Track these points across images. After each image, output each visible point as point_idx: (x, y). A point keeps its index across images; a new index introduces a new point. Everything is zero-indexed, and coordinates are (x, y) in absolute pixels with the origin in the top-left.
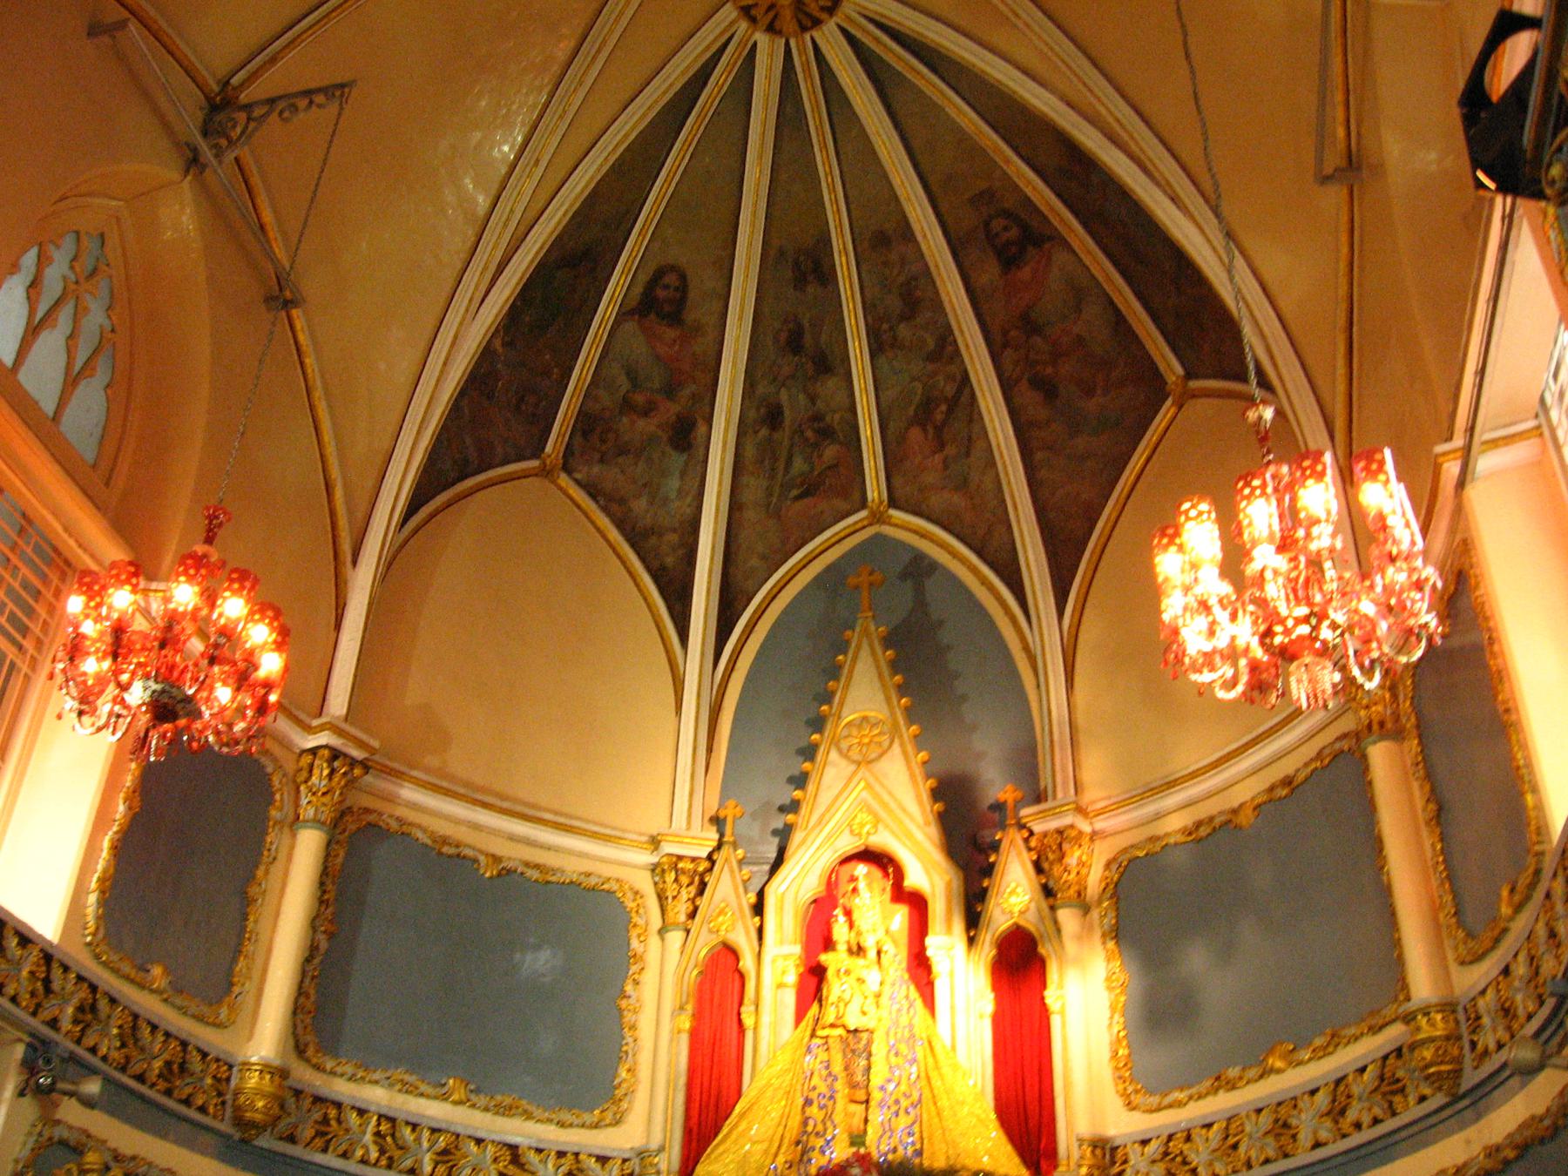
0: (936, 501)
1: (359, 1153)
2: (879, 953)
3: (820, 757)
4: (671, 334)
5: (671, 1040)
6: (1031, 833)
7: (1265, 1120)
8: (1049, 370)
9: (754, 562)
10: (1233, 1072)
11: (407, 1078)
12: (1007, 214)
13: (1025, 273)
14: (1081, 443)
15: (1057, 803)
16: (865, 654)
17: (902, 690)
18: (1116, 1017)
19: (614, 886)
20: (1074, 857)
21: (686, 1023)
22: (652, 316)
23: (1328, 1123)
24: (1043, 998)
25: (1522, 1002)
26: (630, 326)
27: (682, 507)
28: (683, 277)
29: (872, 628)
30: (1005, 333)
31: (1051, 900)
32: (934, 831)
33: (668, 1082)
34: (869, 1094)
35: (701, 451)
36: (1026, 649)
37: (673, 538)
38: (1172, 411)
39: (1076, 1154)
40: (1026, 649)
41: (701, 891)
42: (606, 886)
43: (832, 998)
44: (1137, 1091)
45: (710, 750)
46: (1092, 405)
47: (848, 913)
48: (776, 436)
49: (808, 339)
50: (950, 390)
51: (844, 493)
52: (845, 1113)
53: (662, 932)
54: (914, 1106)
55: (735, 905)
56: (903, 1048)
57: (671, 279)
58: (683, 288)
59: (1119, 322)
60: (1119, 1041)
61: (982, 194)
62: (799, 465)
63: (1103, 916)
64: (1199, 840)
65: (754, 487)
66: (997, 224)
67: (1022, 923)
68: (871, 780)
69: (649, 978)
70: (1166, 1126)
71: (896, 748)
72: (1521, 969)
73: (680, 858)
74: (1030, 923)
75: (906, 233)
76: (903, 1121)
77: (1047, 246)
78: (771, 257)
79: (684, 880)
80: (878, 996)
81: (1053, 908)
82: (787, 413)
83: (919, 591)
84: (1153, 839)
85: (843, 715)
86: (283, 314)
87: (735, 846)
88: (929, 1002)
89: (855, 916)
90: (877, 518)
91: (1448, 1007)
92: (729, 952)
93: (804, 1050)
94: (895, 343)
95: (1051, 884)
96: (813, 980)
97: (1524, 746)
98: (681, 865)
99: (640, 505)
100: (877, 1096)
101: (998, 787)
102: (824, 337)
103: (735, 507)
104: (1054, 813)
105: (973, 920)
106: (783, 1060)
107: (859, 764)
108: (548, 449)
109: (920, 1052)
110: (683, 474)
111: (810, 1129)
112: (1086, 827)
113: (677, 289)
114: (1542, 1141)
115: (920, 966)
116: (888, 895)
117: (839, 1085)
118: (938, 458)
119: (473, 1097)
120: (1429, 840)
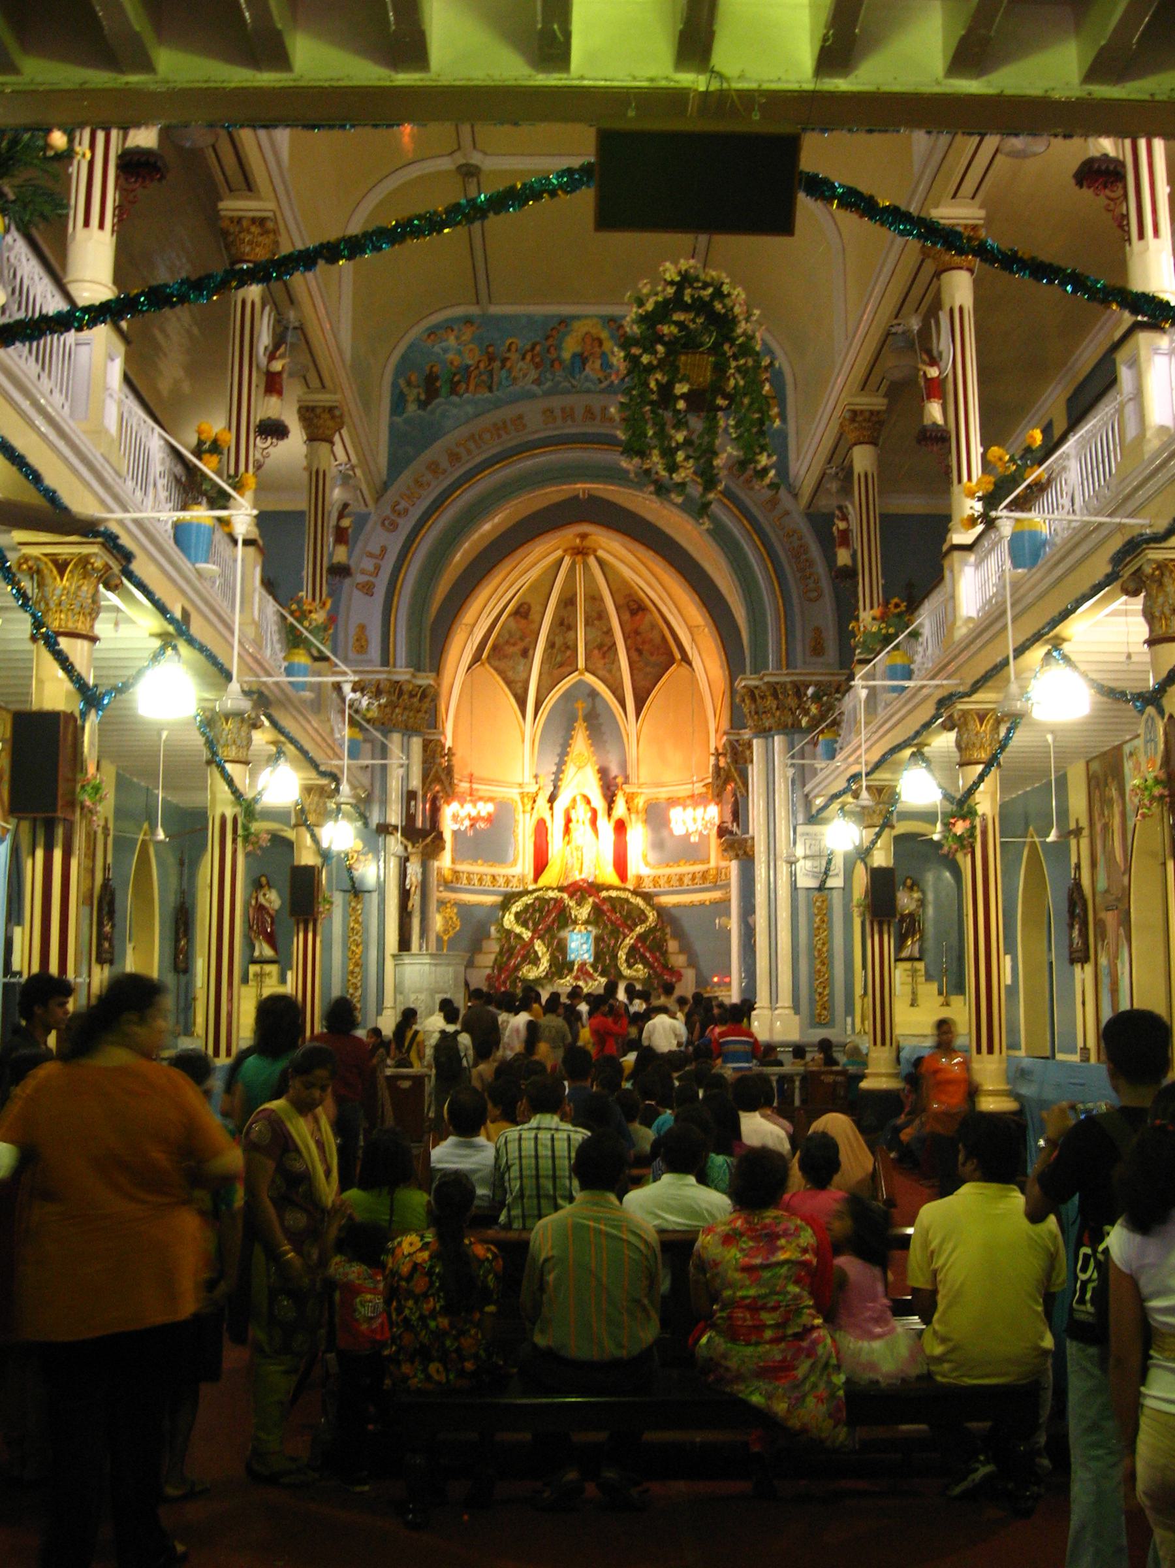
4: (523, 621)
13: (638, 618)
14: (648, 669)
17: (592, 745)
20: (636, 801)
27: (524, 676)
37: (520, 685)
41: (534, 801)
46: (653, 659)
49: (566, 622)
50: (609, 644)
51: (571, 665)
63: (642, 816)
65: (546, 667)
66: (631, 603)
75: (602, 600)
83: (594, 704)
90: (581, 674)
94: (593, 625)
96: (567, 830)
99: (510, 674)
101: (614, 770)
105: (609, 815)
118: (602, 662)
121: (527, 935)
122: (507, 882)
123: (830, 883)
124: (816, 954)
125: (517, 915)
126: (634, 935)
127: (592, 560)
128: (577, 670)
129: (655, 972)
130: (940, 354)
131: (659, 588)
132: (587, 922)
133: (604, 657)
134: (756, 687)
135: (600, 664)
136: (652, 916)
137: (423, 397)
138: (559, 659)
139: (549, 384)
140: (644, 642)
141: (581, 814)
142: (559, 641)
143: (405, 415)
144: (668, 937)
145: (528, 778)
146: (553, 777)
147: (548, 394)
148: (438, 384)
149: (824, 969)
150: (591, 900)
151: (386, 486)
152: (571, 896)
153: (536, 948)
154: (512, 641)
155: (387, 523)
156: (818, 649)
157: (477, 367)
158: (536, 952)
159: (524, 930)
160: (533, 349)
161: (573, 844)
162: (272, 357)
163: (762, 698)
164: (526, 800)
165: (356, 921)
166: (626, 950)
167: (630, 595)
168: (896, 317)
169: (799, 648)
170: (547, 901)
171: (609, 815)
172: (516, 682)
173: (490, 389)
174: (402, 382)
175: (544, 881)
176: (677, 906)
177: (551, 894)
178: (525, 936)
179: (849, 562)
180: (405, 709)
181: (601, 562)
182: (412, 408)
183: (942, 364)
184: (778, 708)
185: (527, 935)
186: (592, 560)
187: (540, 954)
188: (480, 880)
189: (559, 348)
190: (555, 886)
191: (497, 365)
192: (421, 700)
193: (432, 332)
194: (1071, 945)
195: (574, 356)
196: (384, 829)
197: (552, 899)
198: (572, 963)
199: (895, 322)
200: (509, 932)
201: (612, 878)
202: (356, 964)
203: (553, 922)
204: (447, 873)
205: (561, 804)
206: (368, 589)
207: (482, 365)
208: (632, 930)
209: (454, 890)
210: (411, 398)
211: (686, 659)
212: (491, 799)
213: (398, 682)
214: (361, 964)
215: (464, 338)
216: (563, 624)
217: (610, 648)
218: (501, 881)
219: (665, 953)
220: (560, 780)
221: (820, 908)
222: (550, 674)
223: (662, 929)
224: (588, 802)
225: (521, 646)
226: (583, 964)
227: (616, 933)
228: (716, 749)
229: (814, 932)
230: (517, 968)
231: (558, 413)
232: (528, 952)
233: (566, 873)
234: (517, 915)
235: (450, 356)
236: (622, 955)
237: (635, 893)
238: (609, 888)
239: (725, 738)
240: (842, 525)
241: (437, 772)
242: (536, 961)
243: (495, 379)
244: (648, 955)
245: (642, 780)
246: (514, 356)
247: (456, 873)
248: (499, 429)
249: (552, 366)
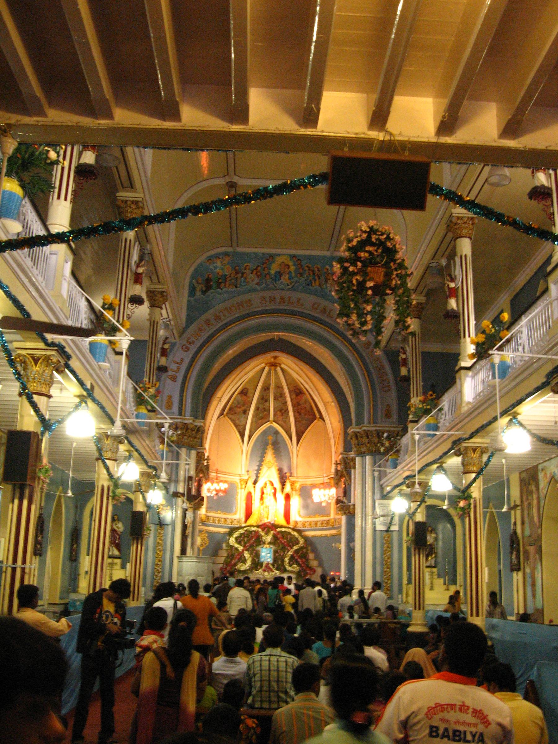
7: (314, 523)
13: (299, 397)
14: (304, 422)
17: (275, 457)
21: (245, 502)
27: (243, 423)
41: (246, 483)
46: (306, 416)
51: (266, 418)
52: (266, 516)
58: (247, 391)
63: (298, 492)
65: (255, 419)
75: (282, 388)
83: (277, 437)
90: (271, 423)
96: (262, 498)
99: (237, 422)
101: (285, 470)
105: (282, 491)
121: (241, 548)
122: (232, 522)
123: (393, 528)
124: (384, 563)
125: (237, 538)
126: (293, 550)
127: (278, 369)
128: (269, 421)
130: (455, 276)
131: (311, 384)
132: (270, 543)
133: (282, 415)
134: (358, 432)
135: (280, 418)
136: (302, 541)
137: (204, 289)
138: (261, 415)
139: (264, 285)
140: (302, 409)
141: (269, 490)
142: (261, 407)
143: (196, 297)
145: (244, 472)
146: (256, 472)
147: (264, 290)
148: (211, 283)
149: (388, 570)
150: (272, 532)
151: (185, 330)
152: (263, 530)
153: (245, 555)
155: (184, 347)
156: (388, 415)
157: (230, 276)
158: (244, 557)
160: (256, 269)
161: (264, 505)
162: (138, 266)
163: (361, 437)
164: (242, 482)
165: (161, 540)
166: (288, 558)
168: (433, 259)
169: (379, 413)
170: (251, 532)
171: (282, 491)
172: (239, 425)
173: (236, 287)
174: (194, 281)
175: (250, 522)
176: (314, 537)
177: (253, 529)
178: (239, 549)
179: (406, 374)
180: (189, 437)
181: (282, 369)
182: (198, 294)
183: (456, 281)
184: (368, 443)
185: (241, 548)
186: (278, 369)
187: (247, 558)
188: (219, 521)
189: (269, 269)
190: (255, 524)
191: (240, 275)
192: (197, 433)
193: (210, 259)
194: (511, 563)
195: (276, 272)
196: (176, 495)
197: (254, 531)
198: (262, 563)
199: (433, 261)
200: (232, 547)
201: (282, 522)
202: (160, 561)
204: (203, 517)
205: (259, 485)
206: (174, 379)
207: (232, 275)
208: (292, 548)
209: (205, 525)
210: (198, 289)
211: (321, 417)
212: (226, 482)
213: (186, 424)
214: (162, 561)
215: (225, 262)
216: (264, 399)
217: (285, 411)
218: (229, 521)
219: (307, 560)
220: (259, 473)
221: (386, 540)
222: (256, 422)
223: (306, 548)
224: (272, 485)
225: (243, 408)
226: (268, 564)
227: (284, 549)
228: (336, 461)
229: (384, 552)
230: (235, 565)
231: (267, 299)
233: (260, 518)
235: (217, 270)
236: (287, 560)
237: (294, 530)
238: (281, 527)
239: (341, 456)
240: (403, 356)
241: (201, 468)
242: (244, 561)
243: (239, 282)
244: (299, 560)
245: (299, 475)
246: (248, 272)
247: (207, 517)
248: (239, 305)
249: (265, 277)
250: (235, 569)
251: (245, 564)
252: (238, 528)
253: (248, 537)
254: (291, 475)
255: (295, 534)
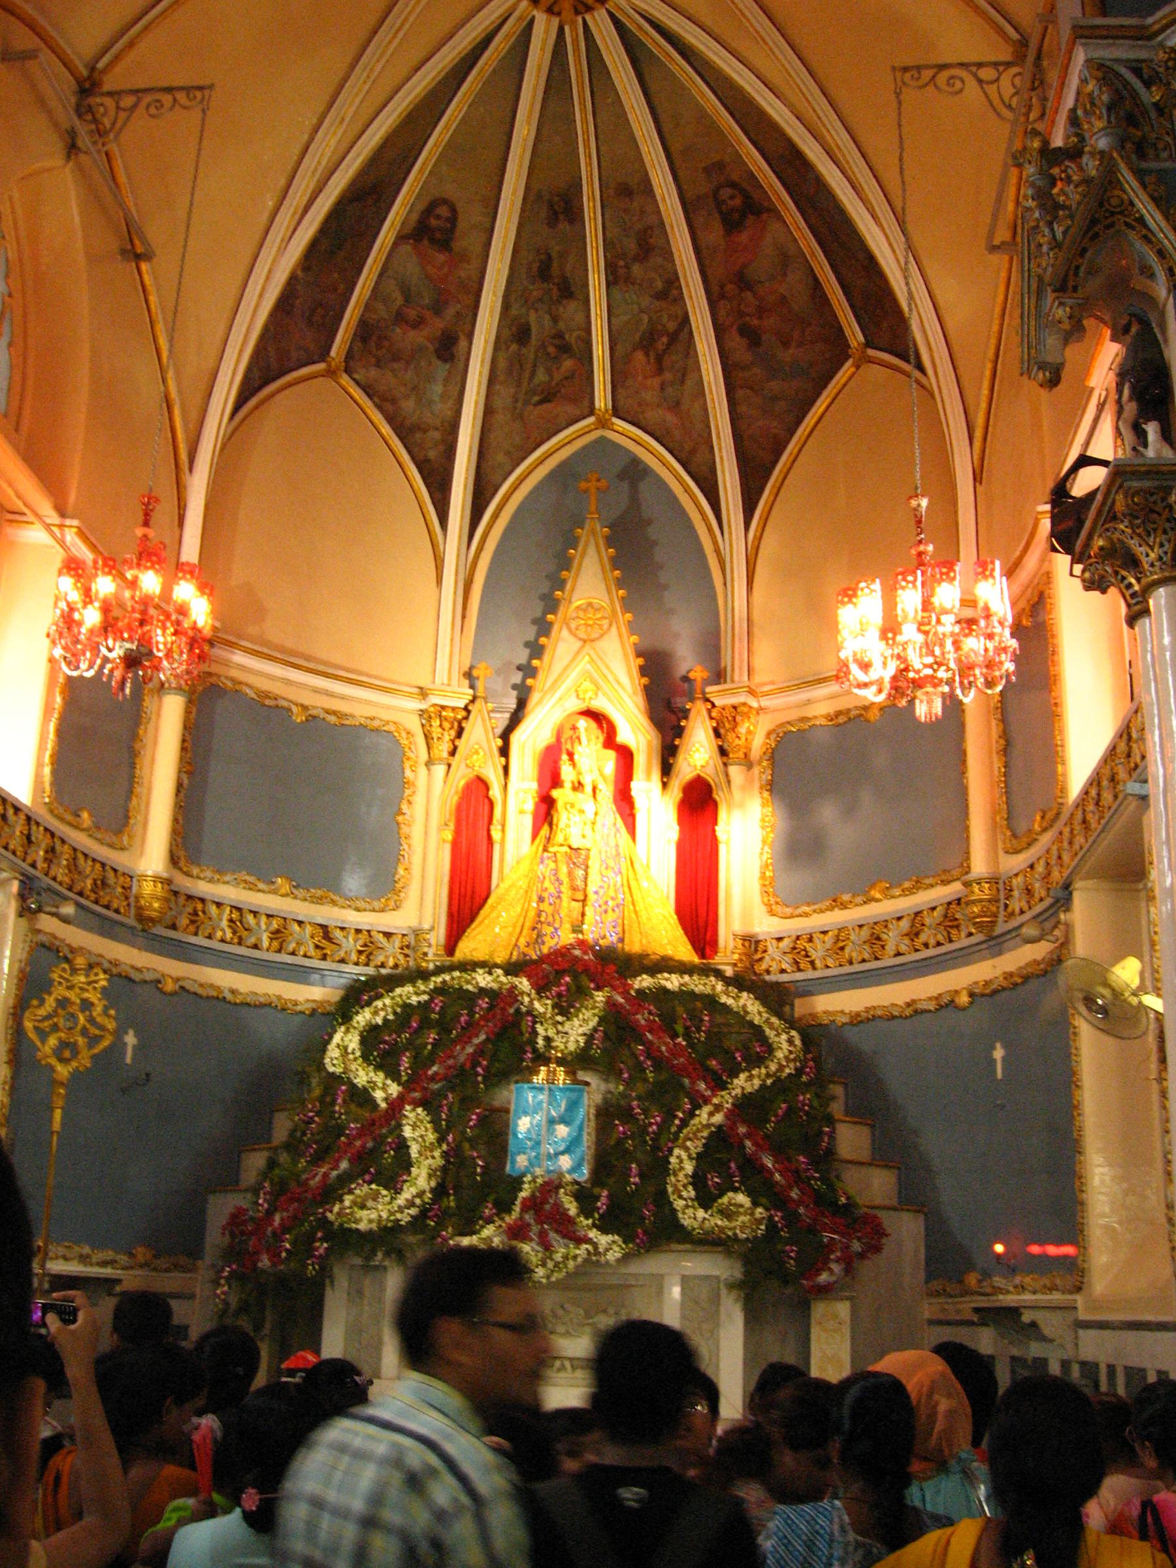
0: (653, 416)
1: (219, 934)
2: (594, 789)
3: (554, 633)
4: (441, 258)
5: (438, 849)
6: (714, 706)
7: (865, 933)
8: (755, 322)
9: (500, 458)
10: (846, 897)
11: (248, 878)
12: (733, 185)
13: (744, 238)
14: (775, 386)
15: (734, 686)
16: (592, 550)
17: (620, 583)
18: (767, 849)
19: (391, 728)
20: (742, 730)
21: (449, 835)
22: (426, 242)
23: (907, 941)
24: (714, 831)
25: (1038, 889)
26: (406, 248)
27: (443, 409)
28: (454, 211)
29: (598, 527)
30: (722, 287)
31: (725, 759)
32: (640, 700)
33: (436, 880)
34: (586, 896)
35: (461, 365)
36: (717, 551)
37: (436, 435)
38: (853, 369)
39: (731, 944)
40: (717, 551)
41: (459, 734)
42: (386, 728)
43: (561, 825)
44: (777, 903)
45: (464, 617)
46: (787, 355)
47: (571, 755)
48: (524, 351)
49: (555, 271)
50: (671, 326)
51: (574, 400)
52: (569, 908)
53: (429, 763)
54: (618, 906)
55: (485, 745)
56: (611, 863)
57: (443, 211)
59: (816, 286)
60: (767, 866)
61: (713, 164)
62: (541, 376)
63: (761, 773)
64: (838, 725)
65: (505, 393)
67: (703, 775)
68: (595, 657)
69: (419, 800)
70: (797, 930)
71: (614, 629)
72: (1040, 868)
73: (443, 707)
74: (709, 775)
76: (611, 916)
77: (765, 216)
78: (531, 198)
79: (446, 725)
80: (594, 823)
81: (725, 764)
82: (534, 330)
84: (804, 719)
85: (573, 599)
86: (134, 265)
87: (485, 699)
88: (631, 829)
89: (576, 757)
90: (603, 424)
91: (993, 880)
92: (479, 785)
93: (538, 860)
95: (726, 746)
96: (546, 809)
97: (1061, 731)
98: (444, 713)
99: (408, 406)
100: (592, 897)
102: (568, 267)
103: (489, 411)
104: (731, 692)
105: (667, 770)
106: (525, 867)
107: (585, 641)
108: (333, 353)
109: (624, 866)
110: (446, 381)
111: (543, 919)
112: (755, 704)
113: (447, 219)
114: (1038, 976)
115: (624, 800)
116: (600, 745)
117: (565, 888)
118: (655, 382)
119: (294, 891)
120: (998, 764)
121: (385, 1090)
125: (370, 1036)
126: (726, 1099)
128: (592, 411)
129: (791, 1218)
132: (577, 1062)
133: (660, 370)
138: (541, 376)
140: (762, 311)
144: (837, 1108)
150: (600, 997)
152: (541, 989)
153: (407, 1132)
154: (412, 314)
158: (402, 1146)
159: (379, 1078)
166: (695, 1147)
167: (720, 166)
170: (468, 999)
176: (857, 1020)
177: (483, 979)
178: (379, 1095)
185: (385, 1090)
197: (483, 991)
198: (516, 1183)
203: (480, 1051)
208: (719, 1085)
219: (826, 1159)
225: (438, 325)
226: (551, 1187)
230: (331, 1193)
232: (380, 1141)
234: (370, 1036)
236: (683, 1162)
237: (739, 982)
238: (665, 965)
244: (769, 1162)
250: (324, 1223)
251: (394, 1186)
252: (392, 982)
253: (444, 1027)
254: (719, 676)
255: (750, 1005)
